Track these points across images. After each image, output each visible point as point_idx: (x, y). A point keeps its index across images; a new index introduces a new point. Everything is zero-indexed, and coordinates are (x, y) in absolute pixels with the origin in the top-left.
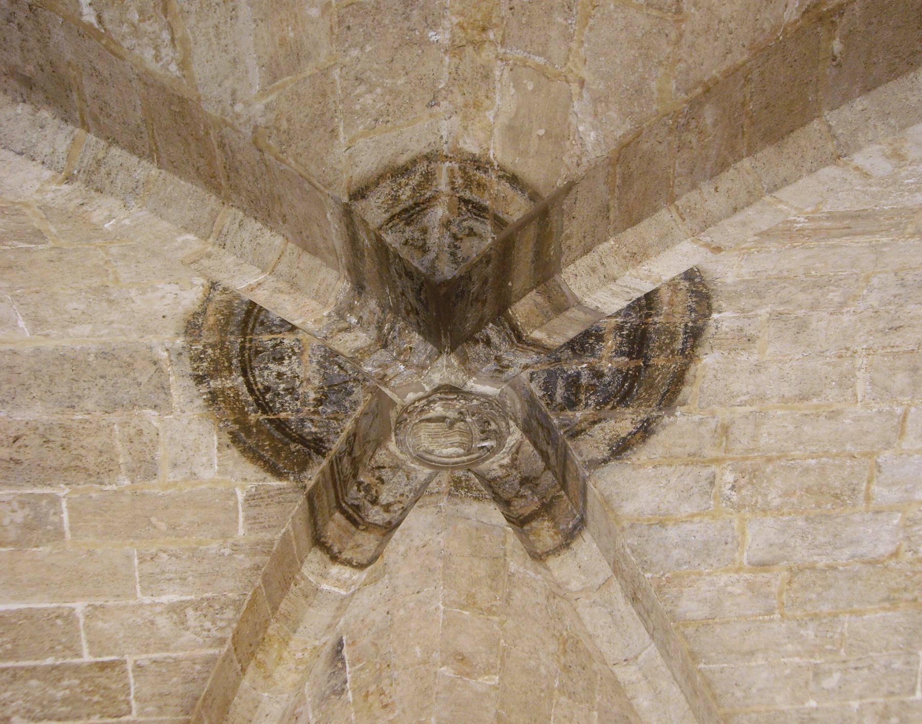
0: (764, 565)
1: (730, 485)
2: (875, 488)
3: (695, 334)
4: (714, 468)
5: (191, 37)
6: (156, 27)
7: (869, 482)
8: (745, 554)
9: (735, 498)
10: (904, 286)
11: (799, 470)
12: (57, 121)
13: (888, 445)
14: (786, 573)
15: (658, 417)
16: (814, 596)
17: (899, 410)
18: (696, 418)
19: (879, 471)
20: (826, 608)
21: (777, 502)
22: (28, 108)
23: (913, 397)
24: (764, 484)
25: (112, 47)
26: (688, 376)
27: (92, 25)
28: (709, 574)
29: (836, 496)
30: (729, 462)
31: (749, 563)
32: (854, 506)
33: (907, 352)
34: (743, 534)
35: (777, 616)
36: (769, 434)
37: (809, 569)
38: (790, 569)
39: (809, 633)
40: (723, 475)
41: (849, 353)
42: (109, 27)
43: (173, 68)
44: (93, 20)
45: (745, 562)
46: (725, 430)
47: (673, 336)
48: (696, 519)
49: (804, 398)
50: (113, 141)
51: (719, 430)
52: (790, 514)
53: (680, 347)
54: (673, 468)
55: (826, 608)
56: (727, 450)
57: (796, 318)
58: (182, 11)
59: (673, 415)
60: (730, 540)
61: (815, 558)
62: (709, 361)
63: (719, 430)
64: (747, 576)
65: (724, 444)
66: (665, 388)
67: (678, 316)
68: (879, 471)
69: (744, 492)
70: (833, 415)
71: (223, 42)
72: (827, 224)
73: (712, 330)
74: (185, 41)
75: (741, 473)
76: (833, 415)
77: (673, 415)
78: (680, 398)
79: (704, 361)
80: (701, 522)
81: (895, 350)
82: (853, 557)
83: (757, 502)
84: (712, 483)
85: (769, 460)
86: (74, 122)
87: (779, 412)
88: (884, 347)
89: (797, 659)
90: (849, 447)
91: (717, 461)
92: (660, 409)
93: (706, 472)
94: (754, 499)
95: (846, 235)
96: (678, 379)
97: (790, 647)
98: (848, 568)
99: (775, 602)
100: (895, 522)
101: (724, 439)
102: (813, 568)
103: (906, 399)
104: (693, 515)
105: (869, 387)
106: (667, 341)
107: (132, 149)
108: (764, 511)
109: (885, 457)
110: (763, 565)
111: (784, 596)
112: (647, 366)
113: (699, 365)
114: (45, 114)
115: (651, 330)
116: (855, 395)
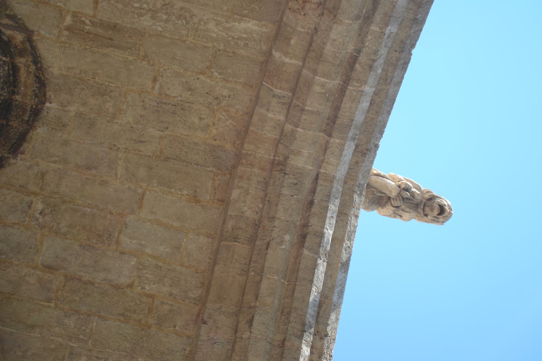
0: (50, 268)
1: (39, 212)
2: (123, 238)
3: (36, 113)
4: (32, 198)
7: (120, 233)
8: (41, 258)
9: (41, 220)
10: (145, 108)
11: (80, 213)
13: (133, 212)
14: (63, 278)
15: (7, 157)
16: (77, 299)
17: (140, 191)
18: (28, 164)
19: (126, 228)
20: (84, 309)
21: (64, 230)
23: (148, 185)
24: (59, 217)
26: (28, 137)
28: (17, 265)
29: (100, 236)
30: (41, 196)
31: (42, 264)
32: (109, 245)
33: (147, 156)
34: (42, 244)
35: (52, 305)
36: (66, 186)
37: (78, 279)
38: (66, 277)
39: (71, 322)
40: (37, 204)
41: (115, 148)
45: (40, 263)
46: (43, 175)
47: (24, 111)
48: (16, 227)
49: (88, 168)
51: (39, 175)
52: (71, 240)
53: (27, 119)
54: (9, 192)
55: (84, 309)
56: (41, 189)
57: (89, 119)
59: (16, 158)
60: (33, 247)
61: (82, 274)
62: (40, 132)
63: (39, 175)
64: (39, 273)
65: (40, 184)
66: (14, 141)
67: (29, 98)
68: (126, 228)
69: (46, 218)
70: (104, 183)
72: (101, 31)
73: (45, 113)
75: (47, 205)
76: (104, 183)
77: (16, 158)
78: (22, 149)
79: (38, 131)
80: (18, 229)
81: (141, 153)
82: (105, 280)
83: (53, 226)
84: (30, 207)
85: (64, 202)
87: (74, 173)
88: (134, 150)
89: (60, 340)
90: (110, 207)
91: (35, 194)
92: (9, 153)
93: (27, 199)
94: (52, 224)
95: (111, 46)
96: (22, 138)
97: (57, 330)
98: (101, 286)
99: (53, 295)
100: (133, 263)
101: (41, 181)
102: (80, 279)
103: (144, 184)
104: (15, 224)
105: (124, 171)
106: (21, 113)
108: (56, 233)
109: (130, 218)
110: (49, 268)
111: (59, 293)
112: (8, 125)
113: (35, 132)
115: (14, 104)
116: (116, 175)
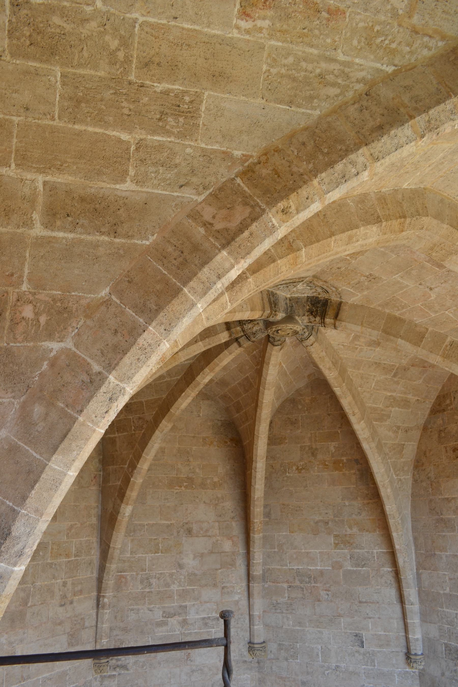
5: (435, 27)
6: (419, 42)
12: (399, 129)
22: (385, 137)
25: (408, 68)
27: (394, 70)
42: (401, 64)
43: (440, 44)
44: (393, 68)
50: (427, 109)
58: (423, 25)
71: (452, 12)
74: (435, 31)
86: (407, 121)
107: (438, 103)
114: (392, 132)
